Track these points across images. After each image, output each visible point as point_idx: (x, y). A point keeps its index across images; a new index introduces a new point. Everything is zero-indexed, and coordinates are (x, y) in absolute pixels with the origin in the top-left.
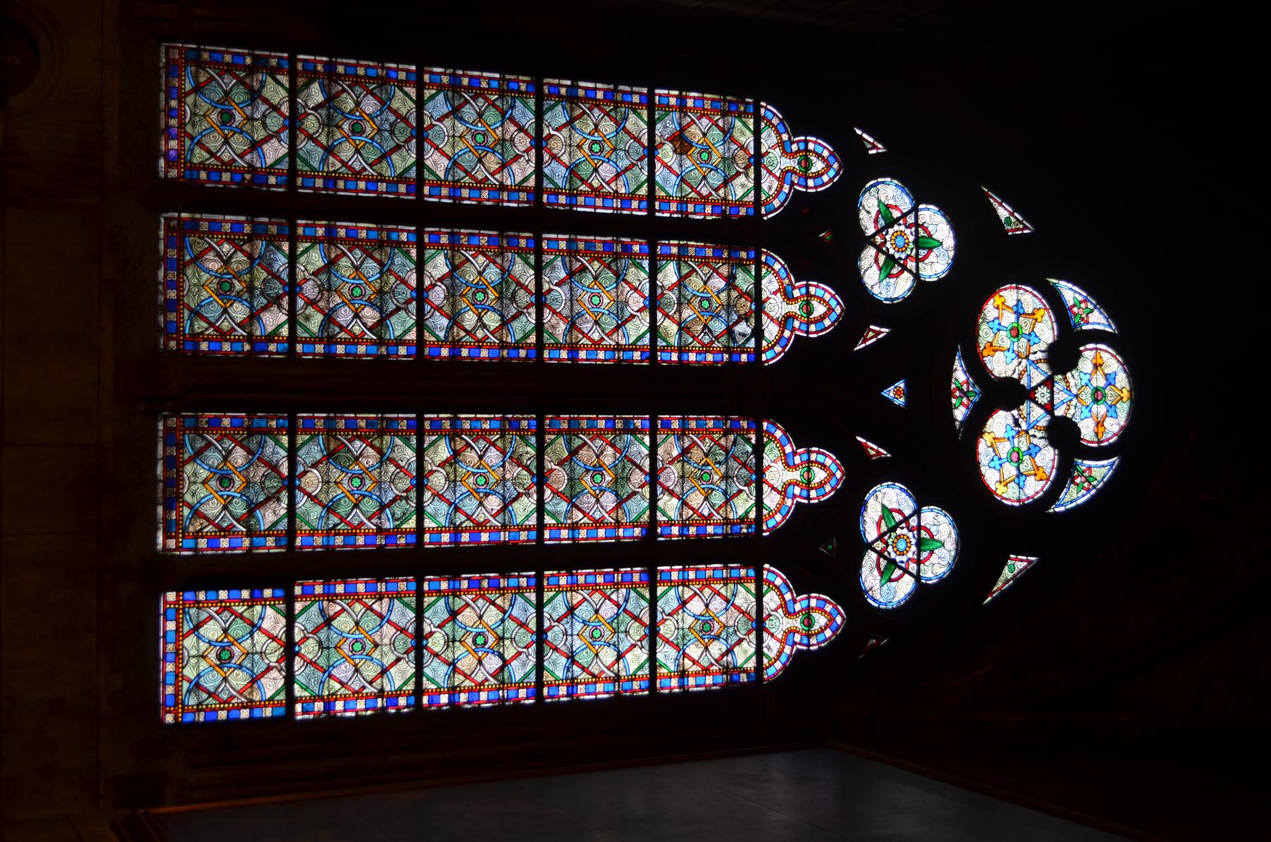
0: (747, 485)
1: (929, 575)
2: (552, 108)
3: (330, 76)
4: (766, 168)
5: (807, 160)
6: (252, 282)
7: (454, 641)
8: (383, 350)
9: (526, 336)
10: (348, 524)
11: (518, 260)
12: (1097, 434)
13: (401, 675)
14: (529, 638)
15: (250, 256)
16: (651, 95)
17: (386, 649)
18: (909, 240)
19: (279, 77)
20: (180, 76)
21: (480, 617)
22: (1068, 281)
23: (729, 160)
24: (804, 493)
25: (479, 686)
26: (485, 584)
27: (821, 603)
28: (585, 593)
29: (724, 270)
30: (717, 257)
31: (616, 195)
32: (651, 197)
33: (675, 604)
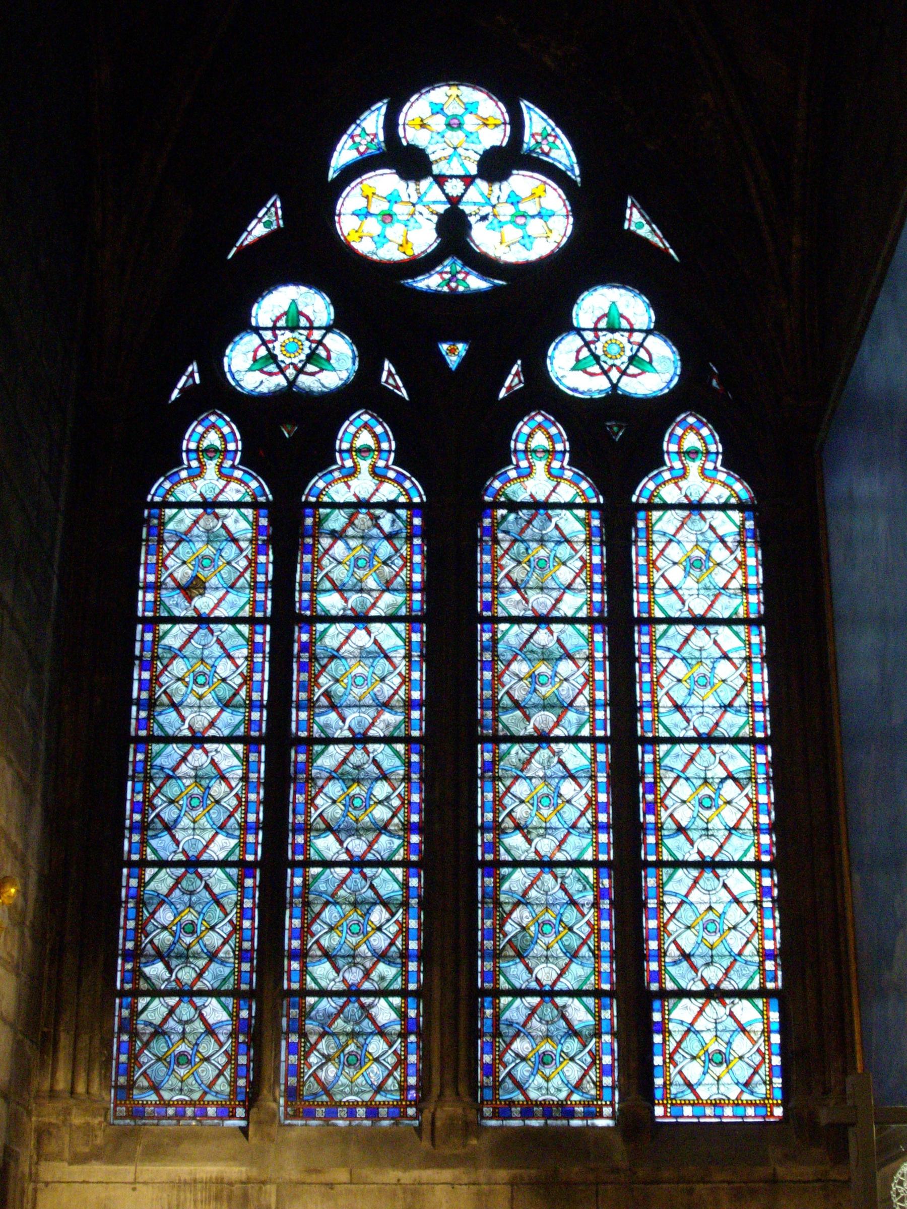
0: (550, 518)
2: (161, 726)
3: (135, 955)
4: (218, 495)
5: (206, 451)
6: (347, 1034)
7: (707, 829)
8: (414, 902)
9: (397, 753)
10: (588, 937)
11: (319, 762)
12: (496, 126)
13: (741, 883)
14: (705, 750)
15: (322, 1036)
16: (144, 620)
17: (714, 899)
19: (140, 1007)
21: (684, 802)
24: (559, 456)
25: (754, 804)
26: (650, 797)
27: (675, 439)
28: (661, 693)
29: (326, 542)
30: (311, 550)
31: (249, 658)
32: (251, 621)
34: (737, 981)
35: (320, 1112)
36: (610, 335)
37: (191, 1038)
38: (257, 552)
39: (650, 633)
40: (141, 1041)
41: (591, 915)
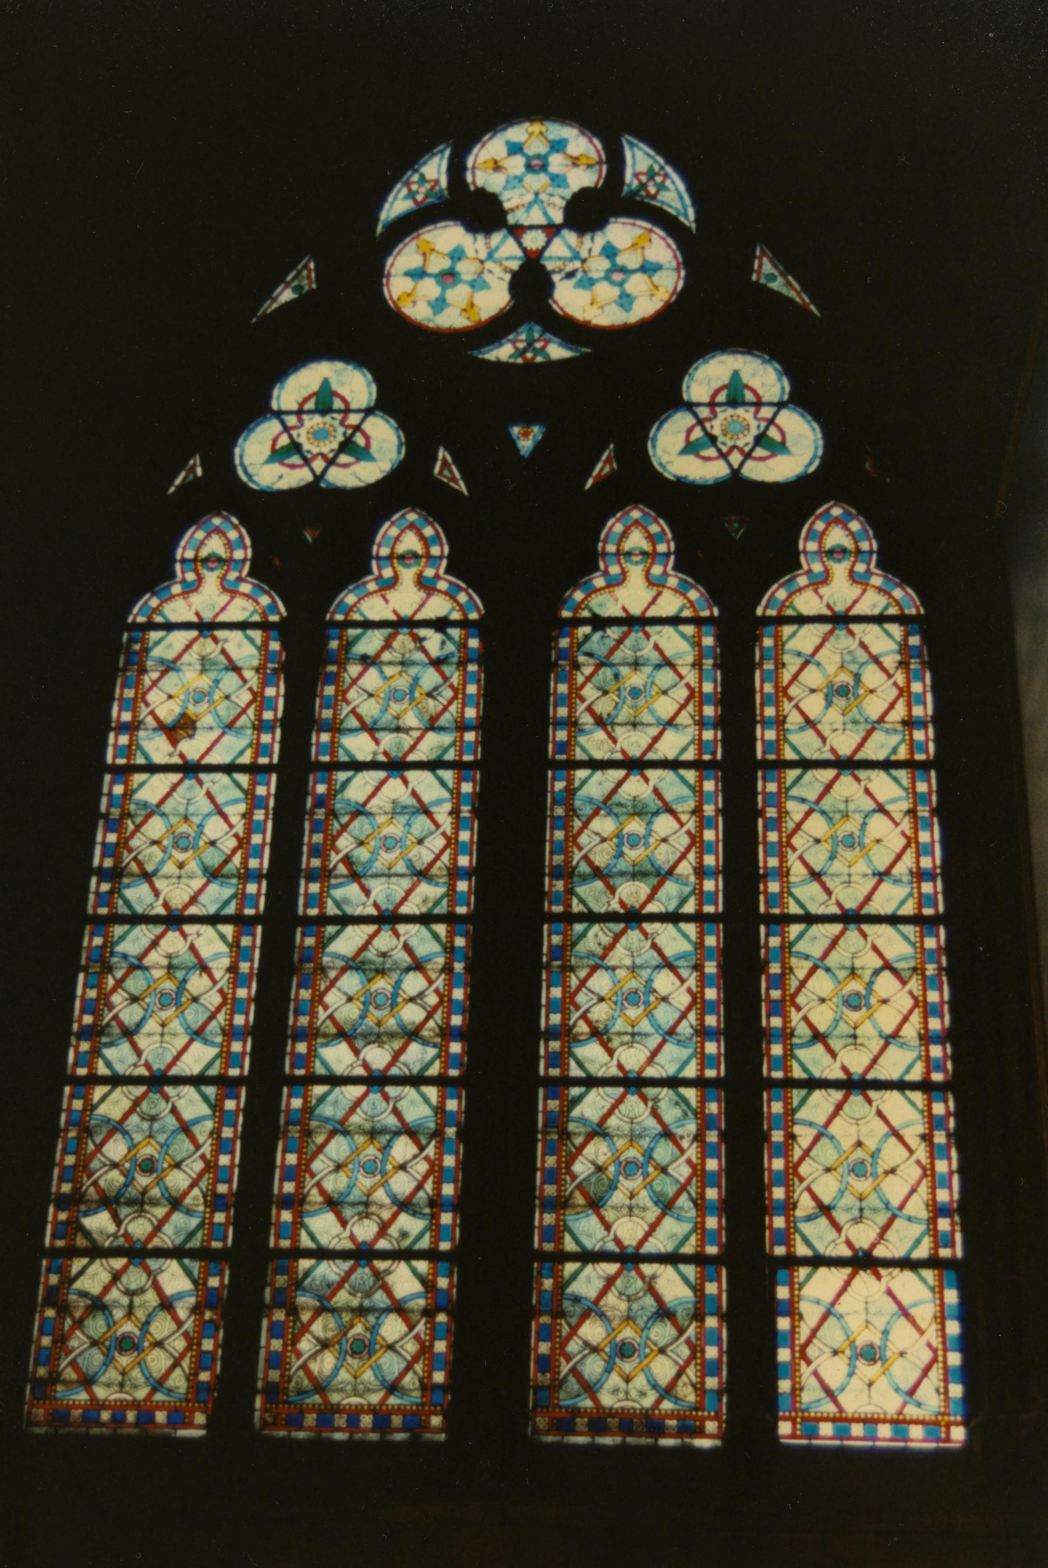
1: (777, 390)
2: (128, 903)
3: (74, 1201)
5: (205, 561)
7: (855, 1037)
15: (318, 1312)
18: (320, 425)
20: (69, 1408)
22: (380, 208)
23: (205, 664)
28: (792, 857)
29: (354, 670)
30: (335, 679)
31: (247, 815)
32: (252, 769)
33: (810, 733)
34: (894, 1247)
35: (310, 1419)
36: (730, 411)
37: (140, 1314)
38: (264, 684)
39: (780, 782)
40: (72, 1317)
41: (692, 1152)
